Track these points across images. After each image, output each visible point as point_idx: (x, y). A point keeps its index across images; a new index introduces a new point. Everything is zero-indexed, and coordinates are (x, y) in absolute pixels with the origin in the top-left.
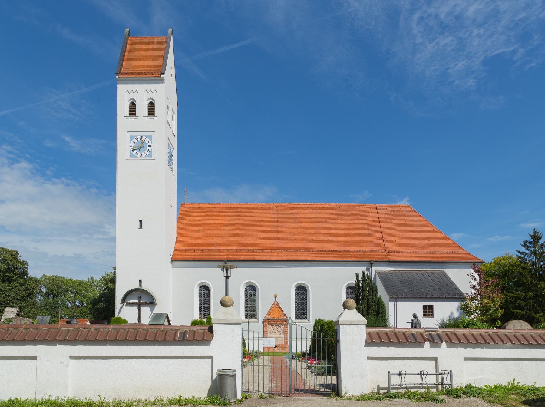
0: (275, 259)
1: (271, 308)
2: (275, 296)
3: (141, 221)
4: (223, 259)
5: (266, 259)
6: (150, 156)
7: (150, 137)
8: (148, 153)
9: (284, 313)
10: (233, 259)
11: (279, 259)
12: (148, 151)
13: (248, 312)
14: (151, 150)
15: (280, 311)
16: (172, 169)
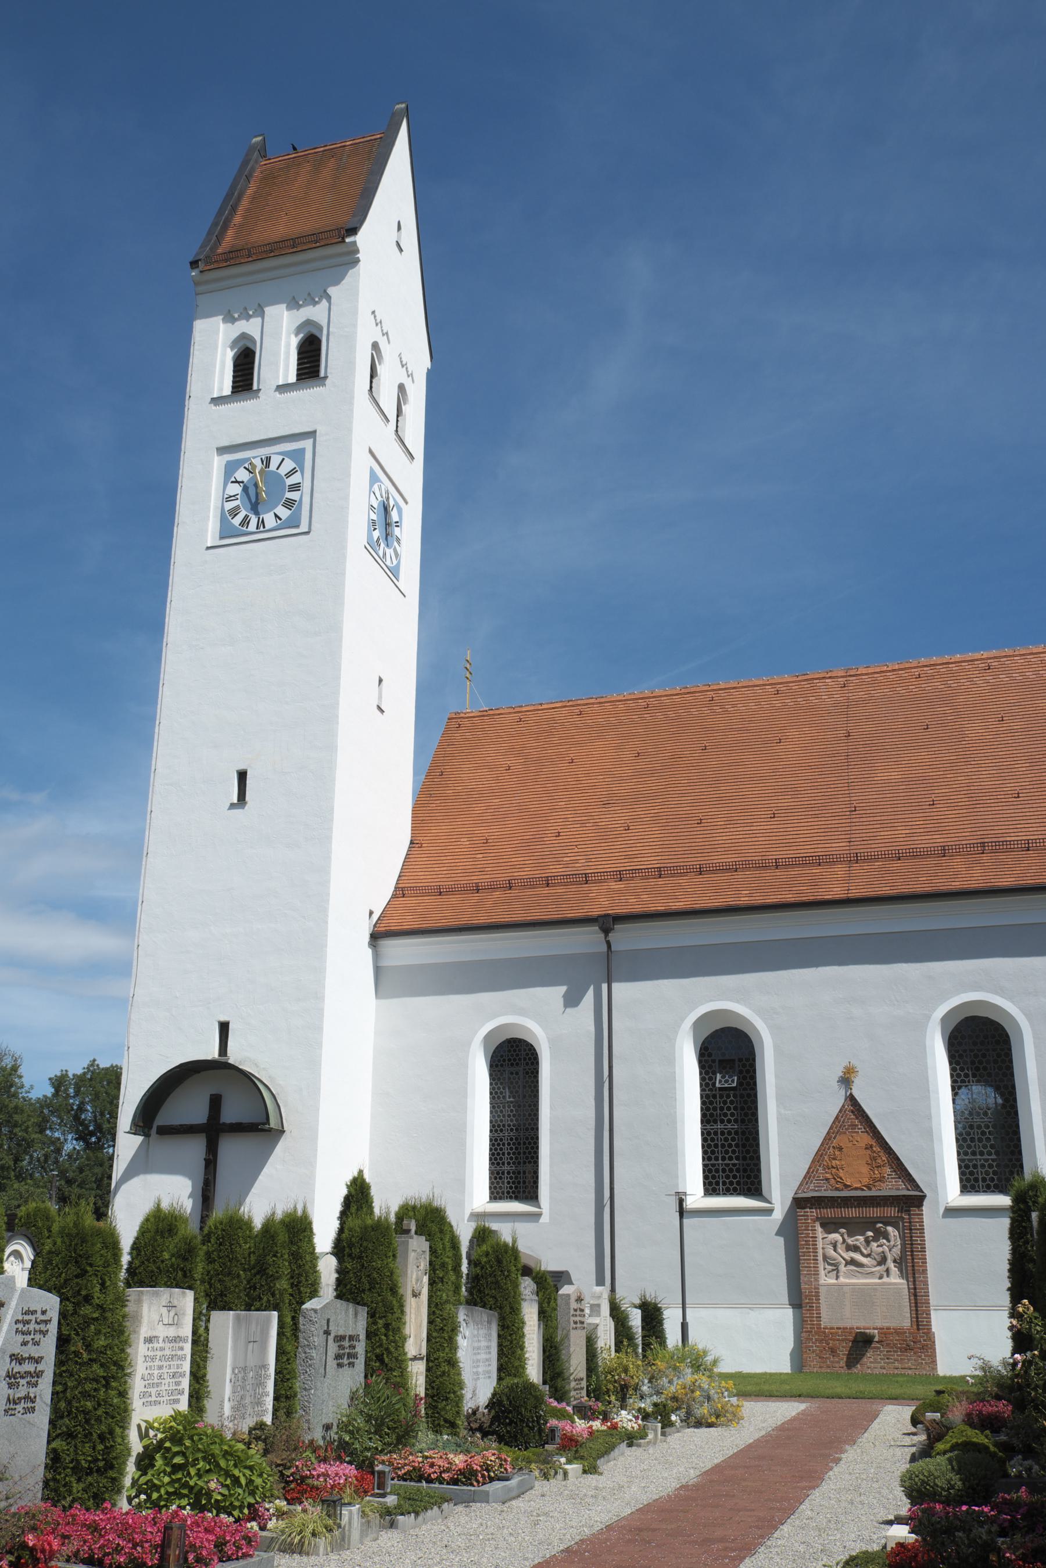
0: (837, 892)
1: (828, 1138)
2: (846, 1080)
3: (242, 776)
4: (596, 913)
5: (790, 898)
6: (293, 522)
7: (297, 456)
8: (289, 512)
9: (898, 1159)
10: (638, 909)
11: (854, 893)
12: (289, 504)
13: (717, 1159)
14: (298, 500)
15: (877, 1149)
16: (394, 573)
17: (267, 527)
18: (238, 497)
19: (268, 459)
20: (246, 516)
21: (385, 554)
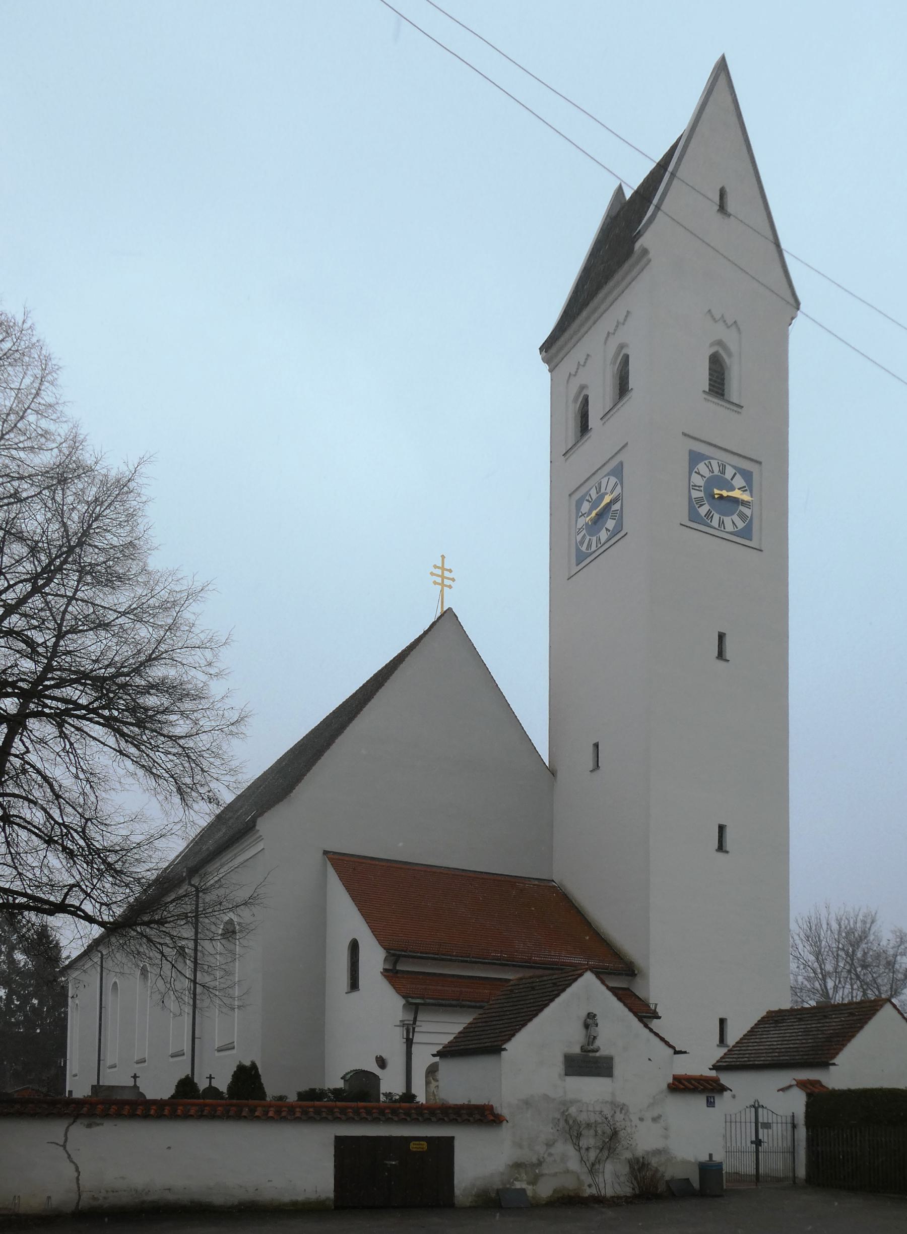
6: (619, 528)
8: (615, 521)
17: (602, 542)
18: (584, 527)
19: (600, 484)
20: (590, 539)
21: (722, 523)
